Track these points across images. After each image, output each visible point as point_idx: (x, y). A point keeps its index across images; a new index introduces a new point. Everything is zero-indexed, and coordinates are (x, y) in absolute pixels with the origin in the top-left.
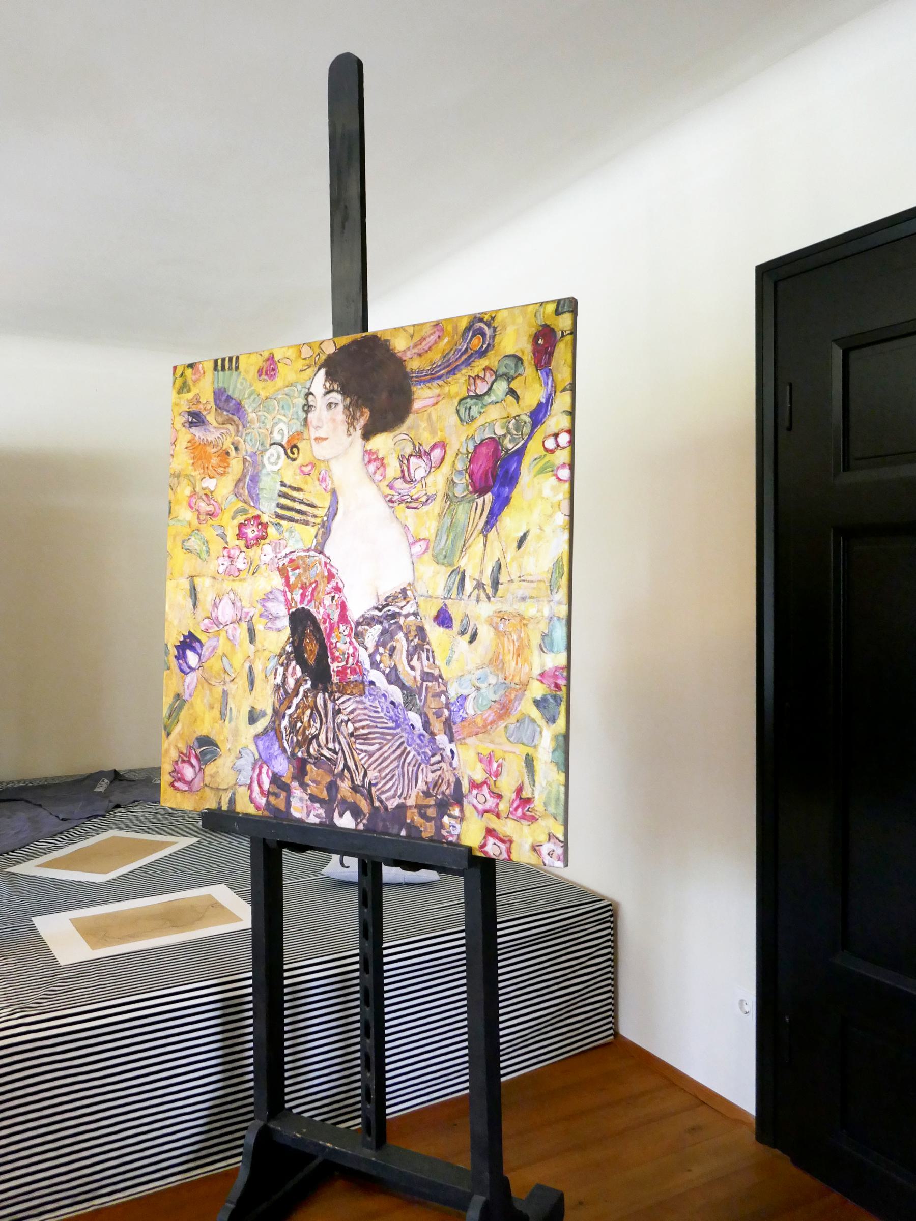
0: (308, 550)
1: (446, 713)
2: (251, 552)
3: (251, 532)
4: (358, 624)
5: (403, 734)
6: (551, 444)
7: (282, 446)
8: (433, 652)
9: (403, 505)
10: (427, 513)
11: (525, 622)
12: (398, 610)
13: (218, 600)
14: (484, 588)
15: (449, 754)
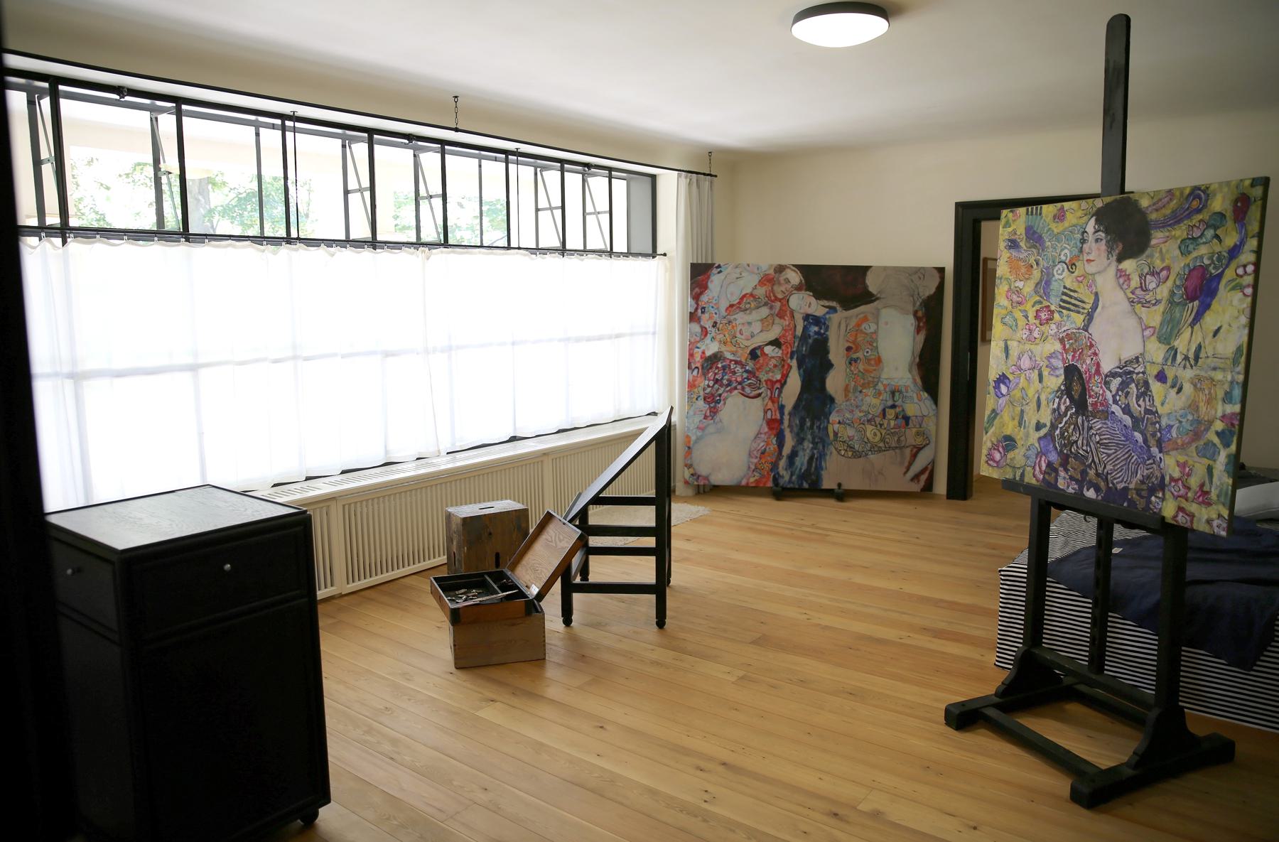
0: (1079, 329)
1: (1159, 434)
2: (1043, 328)
3: (1043, 316)
4: (1107, 376)
9: (1140, 305)
10: (1155, 311)
11: (1214, 383)
12: (1132, 370)
13: (1021, 355)
14: (1189, 361)
15: (1158, 459)
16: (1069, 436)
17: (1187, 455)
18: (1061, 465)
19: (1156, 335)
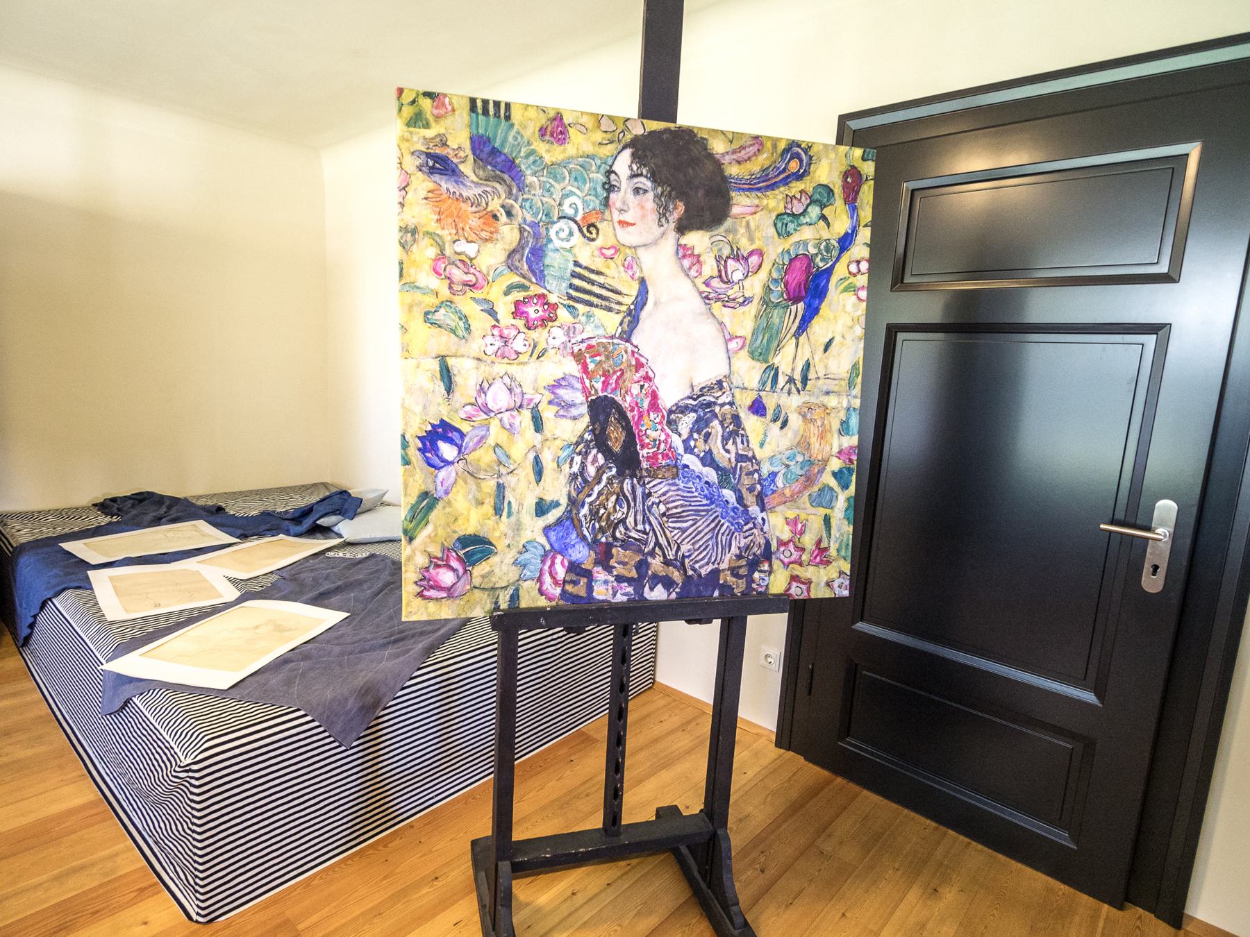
0: (612, 337)
4: (670, 412)
5: (718, 509)
7: (576, 222)
15: (761, 521)
16: (609, 514)
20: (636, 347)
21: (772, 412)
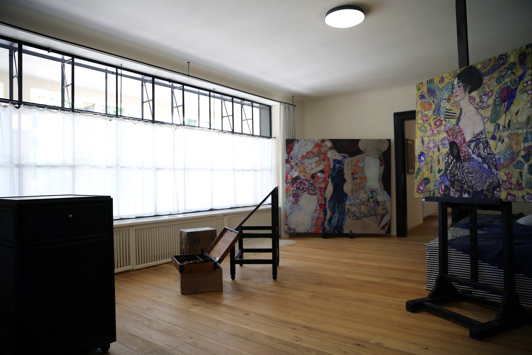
0: (454, 125)
4: (468, 143)
5: (482, 170)
6: (525, 85)
8: (491, 147)
10: (488, 110)
12: (480, 137)
14: (506, 128)
15: (496, 174)
16: (454, 173)
17: (509, 169)
18: (451, 186)
19: (489, 120)
20: (460, 127)
21: (498, 138)
